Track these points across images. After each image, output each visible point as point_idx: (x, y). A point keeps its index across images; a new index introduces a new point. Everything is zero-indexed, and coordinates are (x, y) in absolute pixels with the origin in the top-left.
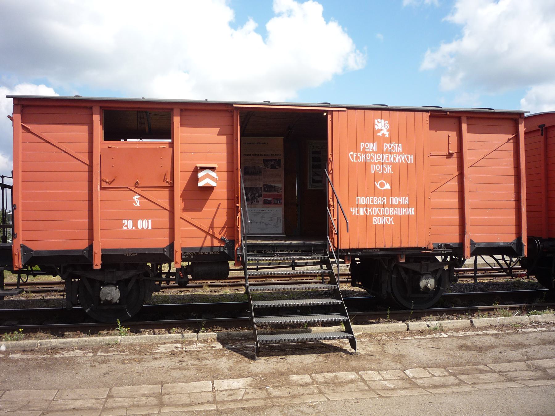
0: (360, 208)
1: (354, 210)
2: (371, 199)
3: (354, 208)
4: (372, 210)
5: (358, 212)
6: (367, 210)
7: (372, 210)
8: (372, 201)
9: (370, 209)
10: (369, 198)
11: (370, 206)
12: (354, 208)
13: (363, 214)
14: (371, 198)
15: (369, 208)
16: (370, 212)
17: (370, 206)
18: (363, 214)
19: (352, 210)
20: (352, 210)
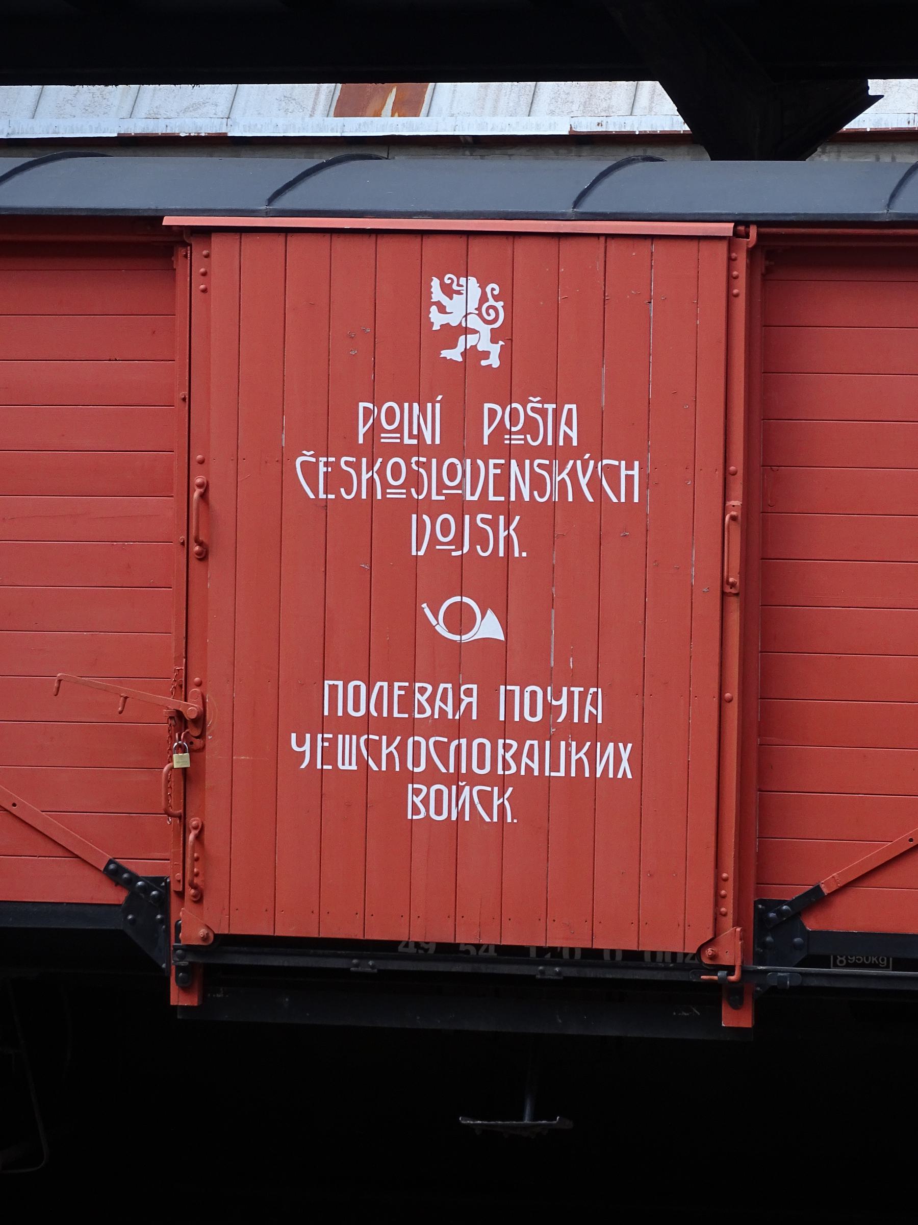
0: (340, 737)
1: (307, 747)
2: (396, 692)
3: (308, 736)
4: (402, 749)
5: (330, 755)
6: (373, 748)
7: (402, 749)
8: (407, 702)
9: (389, 745)
10: (385, 684)
11: (390, 727)
12: (308, 736)
13: (354, 767)
14: (396, 684)
15: (384, 738)
16: (390, 756)
17: (390, 727)
18: (354, 767)
19: (300, 743)
20: (300, 743)
